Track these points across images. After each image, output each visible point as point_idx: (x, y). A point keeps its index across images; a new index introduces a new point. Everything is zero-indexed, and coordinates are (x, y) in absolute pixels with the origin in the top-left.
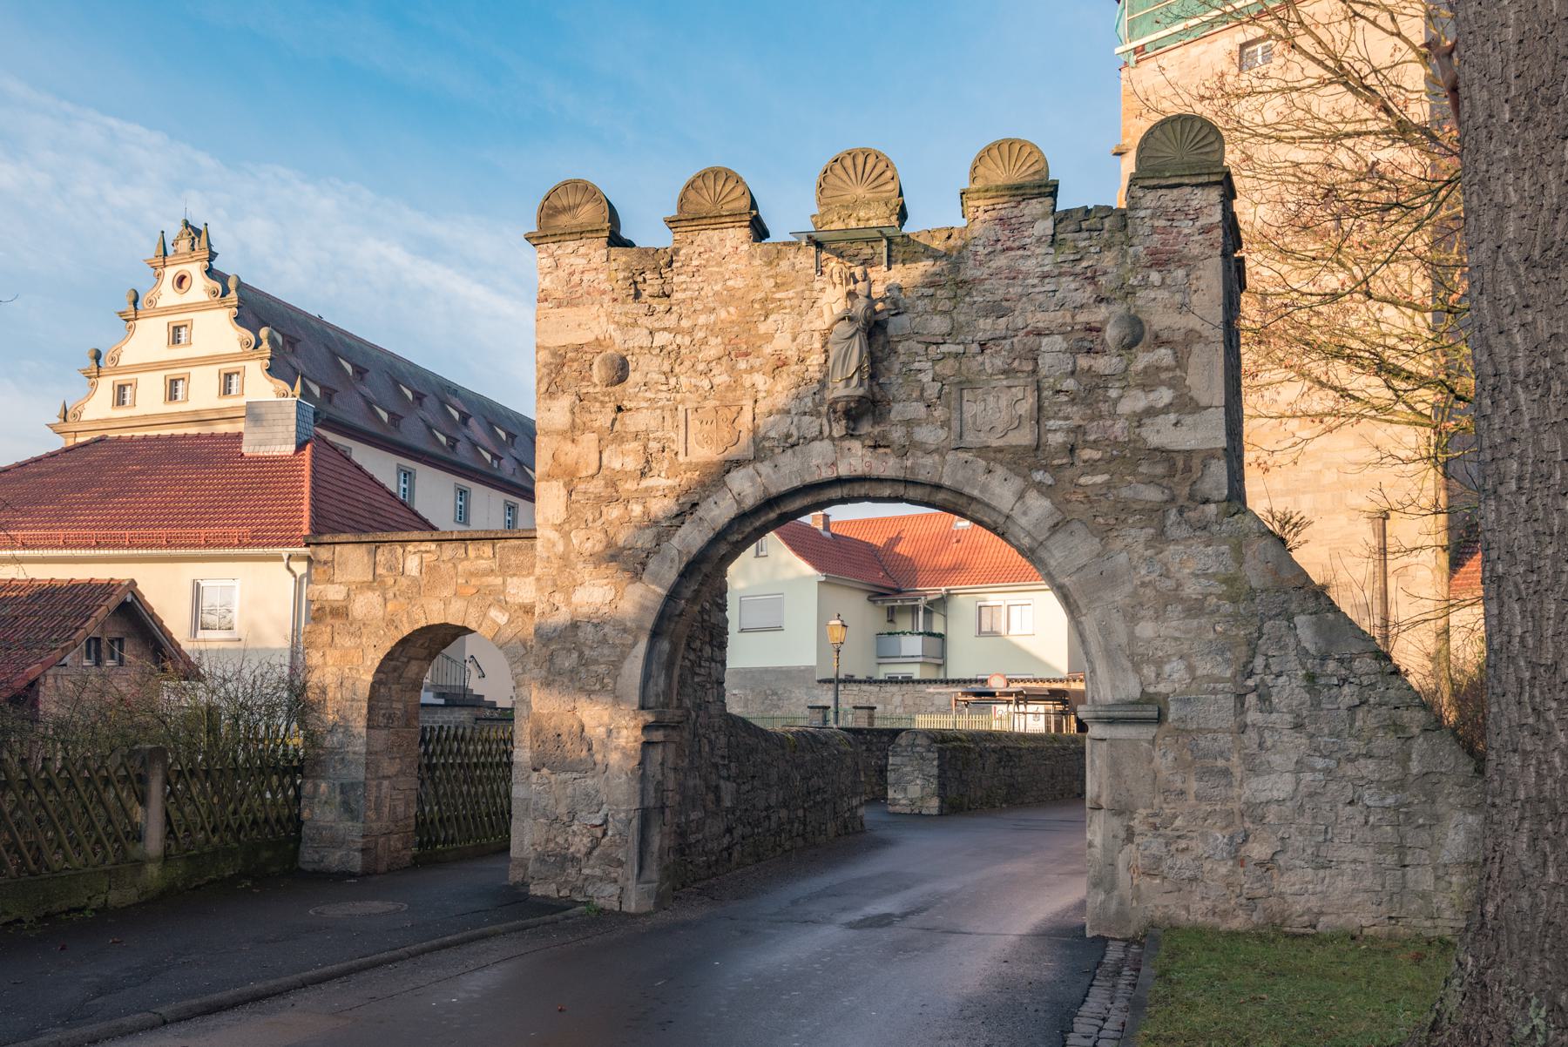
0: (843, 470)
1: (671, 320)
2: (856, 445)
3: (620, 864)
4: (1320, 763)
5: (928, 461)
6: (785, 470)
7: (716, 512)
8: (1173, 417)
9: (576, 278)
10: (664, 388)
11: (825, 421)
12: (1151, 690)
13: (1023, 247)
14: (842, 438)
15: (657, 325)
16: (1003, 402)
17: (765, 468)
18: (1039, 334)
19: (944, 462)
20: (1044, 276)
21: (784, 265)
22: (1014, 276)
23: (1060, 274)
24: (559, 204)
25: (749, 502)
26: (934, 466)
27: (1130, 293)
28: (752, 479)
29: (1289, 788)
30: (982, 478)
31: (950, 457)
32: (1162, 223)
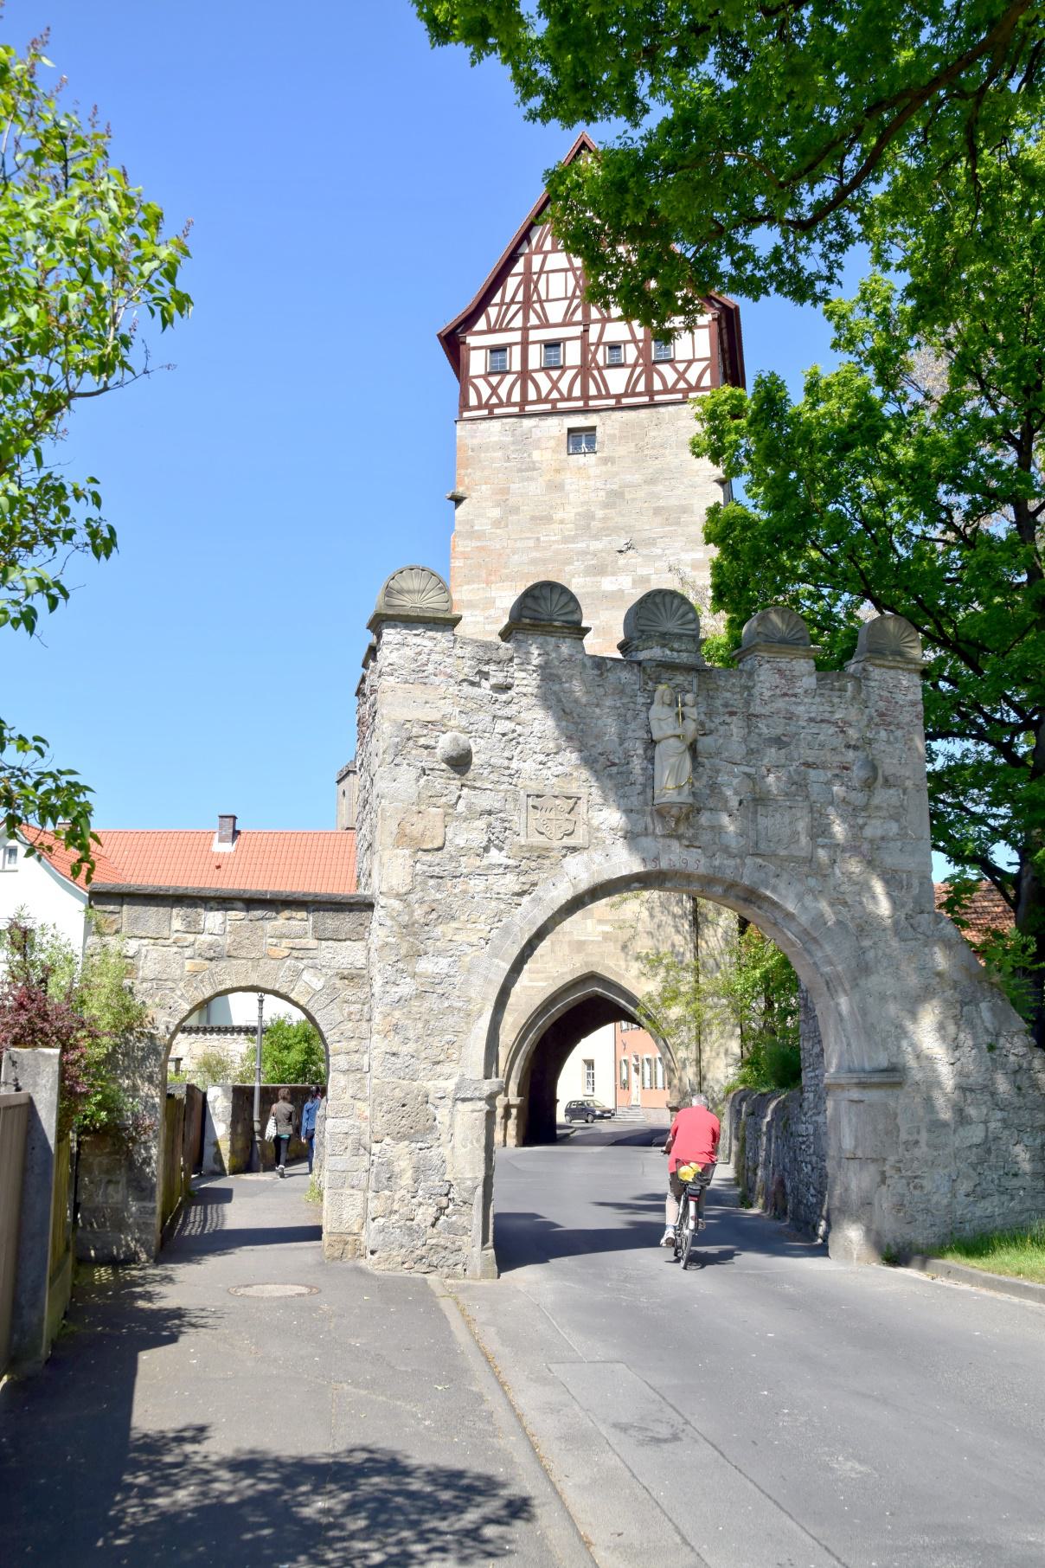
0: (664, 865)
1: (511, 710)
2: (675, 844)
3: (466, 1231)
4: (999, 1115)
5: (731, 862)
6: (615, 860)
7: (554, 893)
8: (899, 844)
9: (424, 657)
10: (507, 772)
11: (649, 820)
12: (894, 1060)
13: (795, 695)
14: (663, 836)
15: (500, 713)
16: (787, 820)
17: (598, 857)
18: (807, 765)
19: (744, 864)
20: (811, 720)
21: (611, 677)
22: (790, 717)
23: (822, 721)
24: (405, 585)
25: (583, 886)
26: (736, 868)
27: (870, 742)
28: (588, 868)
29: (982, 1135)
30: (773, 881)
31: (749, 861)
32: (885, 694)
